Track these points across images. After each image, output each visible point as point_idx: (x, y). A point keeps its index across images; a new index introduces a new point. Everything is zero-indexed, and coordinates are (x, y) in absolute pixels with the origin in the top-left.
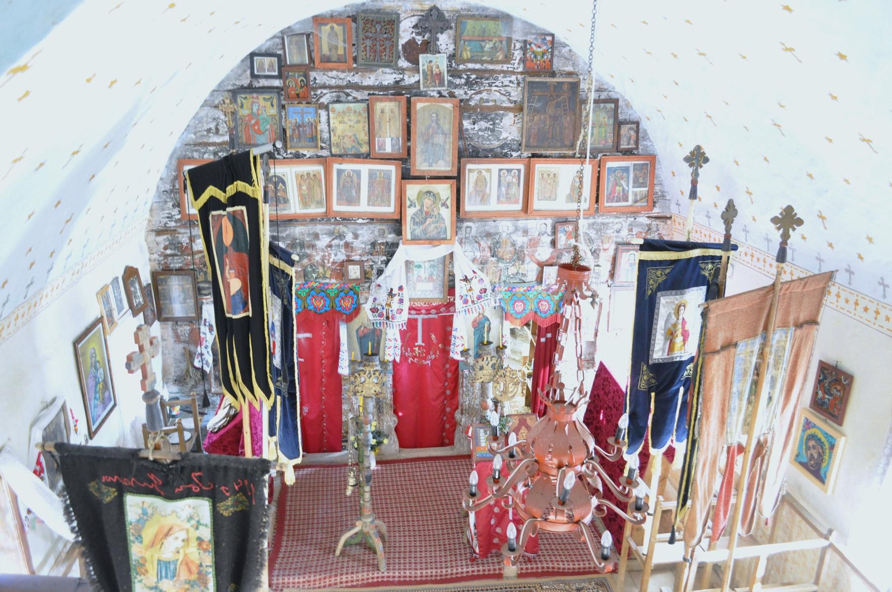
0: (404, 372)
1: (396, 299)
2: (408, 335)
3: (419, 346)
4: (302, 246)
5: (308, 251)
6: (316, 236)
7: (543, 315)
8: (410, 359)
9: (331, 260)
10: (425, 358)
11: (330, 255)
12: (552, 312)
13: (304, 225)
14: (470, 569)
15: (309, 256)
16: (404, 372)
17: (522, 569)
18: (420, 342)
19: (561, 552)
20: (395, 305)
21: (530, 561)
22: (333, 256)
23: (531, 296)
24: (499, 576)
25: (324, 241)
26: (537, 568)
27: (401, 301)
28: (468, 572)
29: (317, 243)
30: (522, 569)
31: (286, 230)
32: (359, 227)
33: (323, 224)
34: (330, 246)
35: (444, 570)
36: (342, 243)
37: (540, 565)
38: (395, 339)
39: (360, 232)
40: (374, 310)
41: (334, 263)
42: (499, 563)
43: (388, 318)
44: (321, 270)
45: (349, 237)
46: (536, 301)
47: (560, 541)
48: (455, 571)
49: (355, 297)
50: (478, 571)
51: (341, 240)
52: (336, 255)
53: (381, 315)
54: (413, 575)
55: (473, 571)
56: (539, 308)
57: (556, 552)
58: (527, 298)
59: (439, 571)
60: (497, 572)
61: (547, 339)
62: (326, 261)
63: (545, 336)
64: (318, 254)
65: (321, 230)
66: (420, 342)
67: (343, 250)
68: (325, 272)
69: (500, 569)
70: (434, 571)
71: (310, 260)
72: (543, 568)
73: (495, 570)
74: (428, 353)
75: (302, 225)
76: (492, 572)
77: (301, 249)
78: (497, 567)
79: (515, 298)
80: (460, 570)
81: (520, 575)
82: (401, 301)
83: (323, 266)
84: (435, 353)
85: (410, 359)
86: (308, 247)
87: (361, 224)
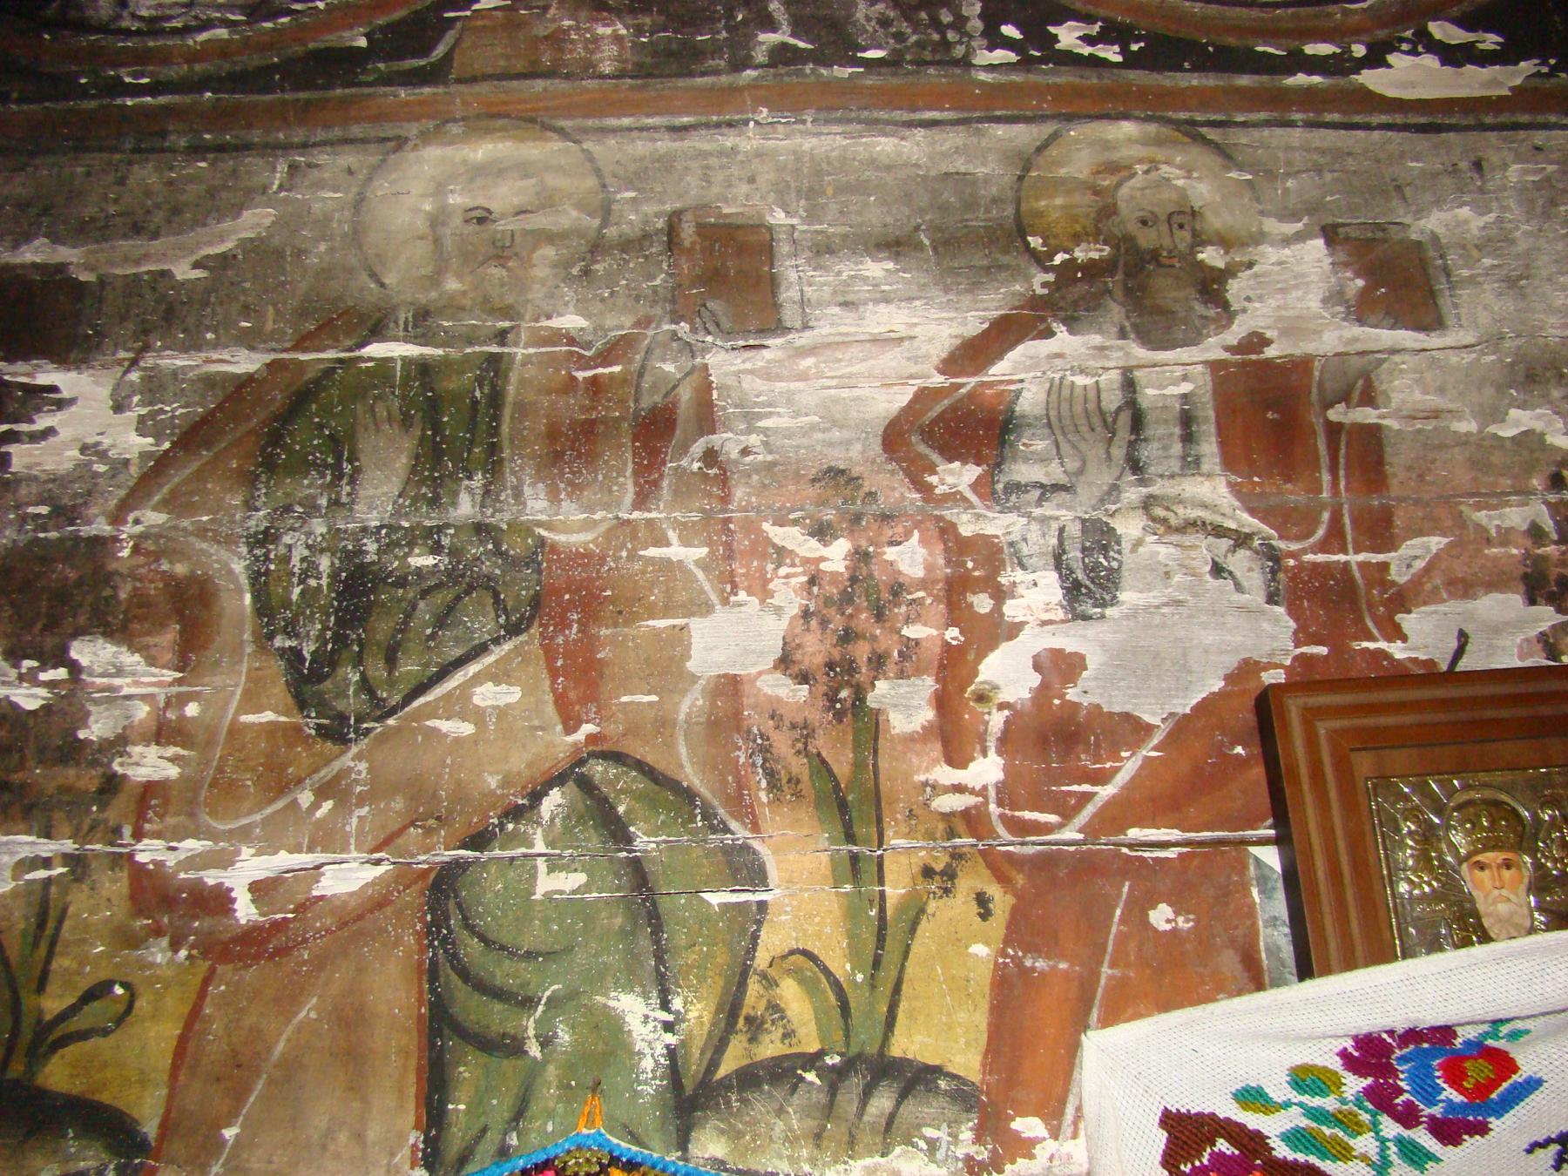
4: (458, 424)
5: (563, 517)
6: (729, 273)
9: (1008, 673)
11: (971, 573)
13: (533, 121)
15: (561, 609)
22: (1036, 595)
25: (861, 346)
29: (724, 363)
31: (221, 202)
32: (1419, 158)
33: (834, 104)
34: (970, 428)
36: (1177, 374)
39: (1445, 221)
41: (1058, 737)
44: (799, 891)
45: (1292, 294)
51: (1156, 326)
52: (1088, 589)
62: (905, 706)
64: (738, 564)
65: (808, 186)
67: (1212, 491)
68: (885, 940)
71: (579, 682)
75: (488, 120)
77: (435, 467)
83: (852, 808)
86: (572, 446)
87: (1429, 118)
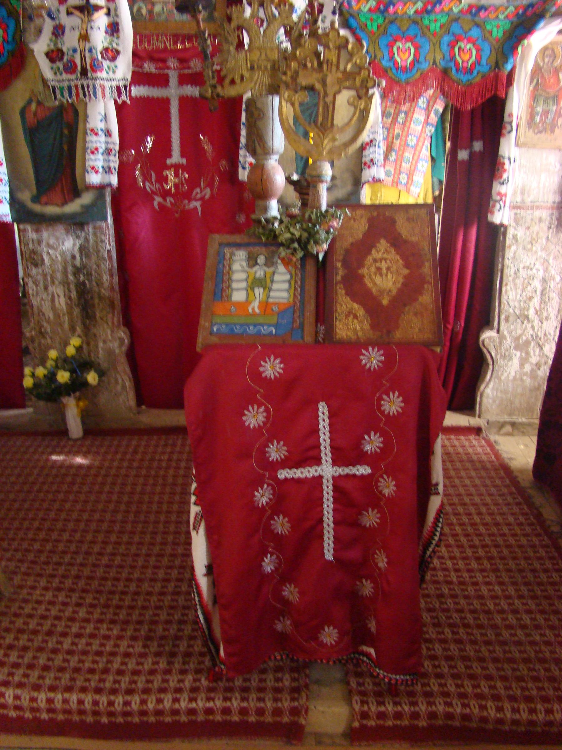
0: (143, 223)
1: (101, 20)
2: (138, 118)
3: (176, 167)
7: (465, 78)
8: (158, 199)
10: (188, 196)
12: (484, 69)
14: (200, 704)
16: (143, 223)
17: (365, 715)
18: (176, 157)
19: (492, 669)
20: (99, 39)
21: (393, 691)
23: (435, 27)
24: (293, 732)
26: (415, 716)
27: (114, 29)
28: (192, 712)
30: (365, 715)
35: (119, 700)
37: (423, 708)
38: (108, 133)
40: (54, 55)
42: (295, 690)
43: (84, 72)
46: (446, 39)
47: (491, 635)
48: (151, 706)
49: (12, 24)
50: (226, 711)
53: (70, 68)
54: (25, 702)
55: (209, 711)
56: (452, 57)
57: (477, 669)
58: (425, 31)
59: (103, 700)
60: (286, 719)
61: (472, 155)
63: (469, 146)
66: (176, 157)
69: (295, 712)
70: (88, 699)
72: (432, 715)
73: (277, 712)
74: (193, 183)
76: (268, 719)
78: (286, 704)
79: (393, 30)
80: (167, 704)
81: (354, 735)
82: (114, 29)
84: (210, 185)
85: (158, 199)
